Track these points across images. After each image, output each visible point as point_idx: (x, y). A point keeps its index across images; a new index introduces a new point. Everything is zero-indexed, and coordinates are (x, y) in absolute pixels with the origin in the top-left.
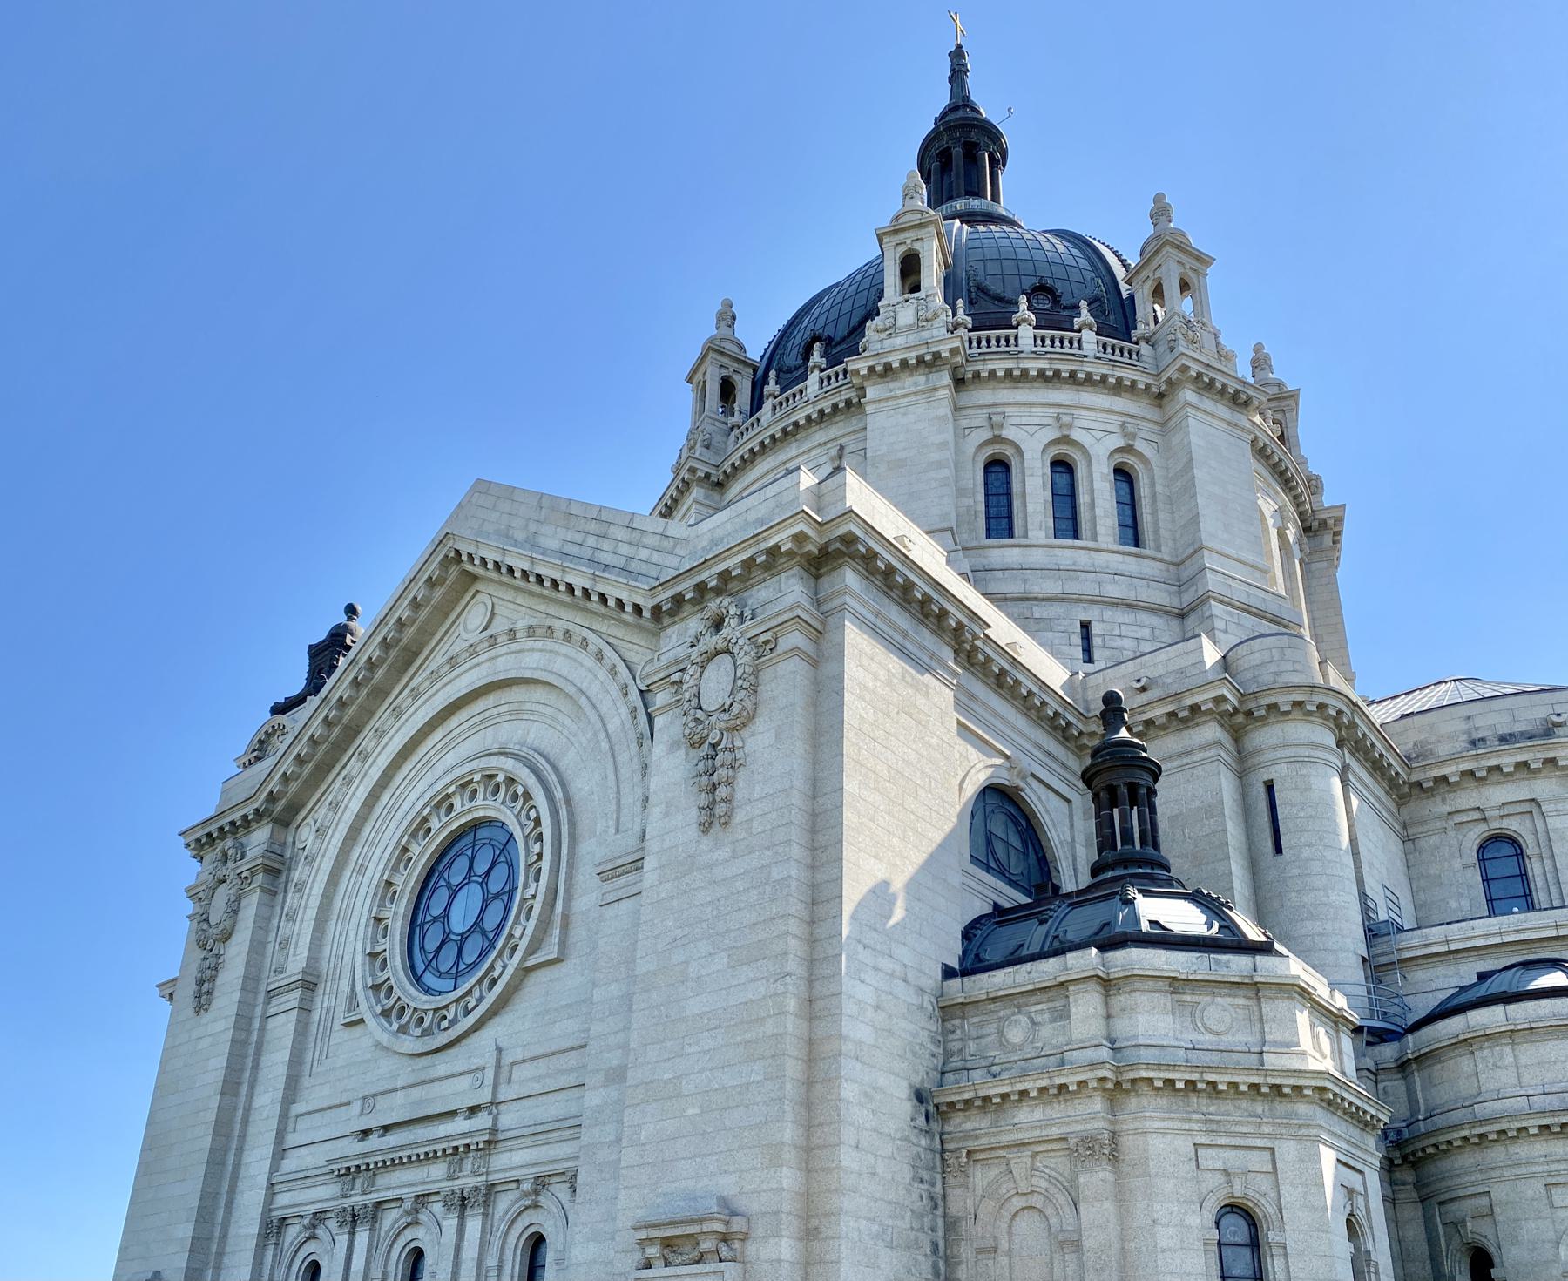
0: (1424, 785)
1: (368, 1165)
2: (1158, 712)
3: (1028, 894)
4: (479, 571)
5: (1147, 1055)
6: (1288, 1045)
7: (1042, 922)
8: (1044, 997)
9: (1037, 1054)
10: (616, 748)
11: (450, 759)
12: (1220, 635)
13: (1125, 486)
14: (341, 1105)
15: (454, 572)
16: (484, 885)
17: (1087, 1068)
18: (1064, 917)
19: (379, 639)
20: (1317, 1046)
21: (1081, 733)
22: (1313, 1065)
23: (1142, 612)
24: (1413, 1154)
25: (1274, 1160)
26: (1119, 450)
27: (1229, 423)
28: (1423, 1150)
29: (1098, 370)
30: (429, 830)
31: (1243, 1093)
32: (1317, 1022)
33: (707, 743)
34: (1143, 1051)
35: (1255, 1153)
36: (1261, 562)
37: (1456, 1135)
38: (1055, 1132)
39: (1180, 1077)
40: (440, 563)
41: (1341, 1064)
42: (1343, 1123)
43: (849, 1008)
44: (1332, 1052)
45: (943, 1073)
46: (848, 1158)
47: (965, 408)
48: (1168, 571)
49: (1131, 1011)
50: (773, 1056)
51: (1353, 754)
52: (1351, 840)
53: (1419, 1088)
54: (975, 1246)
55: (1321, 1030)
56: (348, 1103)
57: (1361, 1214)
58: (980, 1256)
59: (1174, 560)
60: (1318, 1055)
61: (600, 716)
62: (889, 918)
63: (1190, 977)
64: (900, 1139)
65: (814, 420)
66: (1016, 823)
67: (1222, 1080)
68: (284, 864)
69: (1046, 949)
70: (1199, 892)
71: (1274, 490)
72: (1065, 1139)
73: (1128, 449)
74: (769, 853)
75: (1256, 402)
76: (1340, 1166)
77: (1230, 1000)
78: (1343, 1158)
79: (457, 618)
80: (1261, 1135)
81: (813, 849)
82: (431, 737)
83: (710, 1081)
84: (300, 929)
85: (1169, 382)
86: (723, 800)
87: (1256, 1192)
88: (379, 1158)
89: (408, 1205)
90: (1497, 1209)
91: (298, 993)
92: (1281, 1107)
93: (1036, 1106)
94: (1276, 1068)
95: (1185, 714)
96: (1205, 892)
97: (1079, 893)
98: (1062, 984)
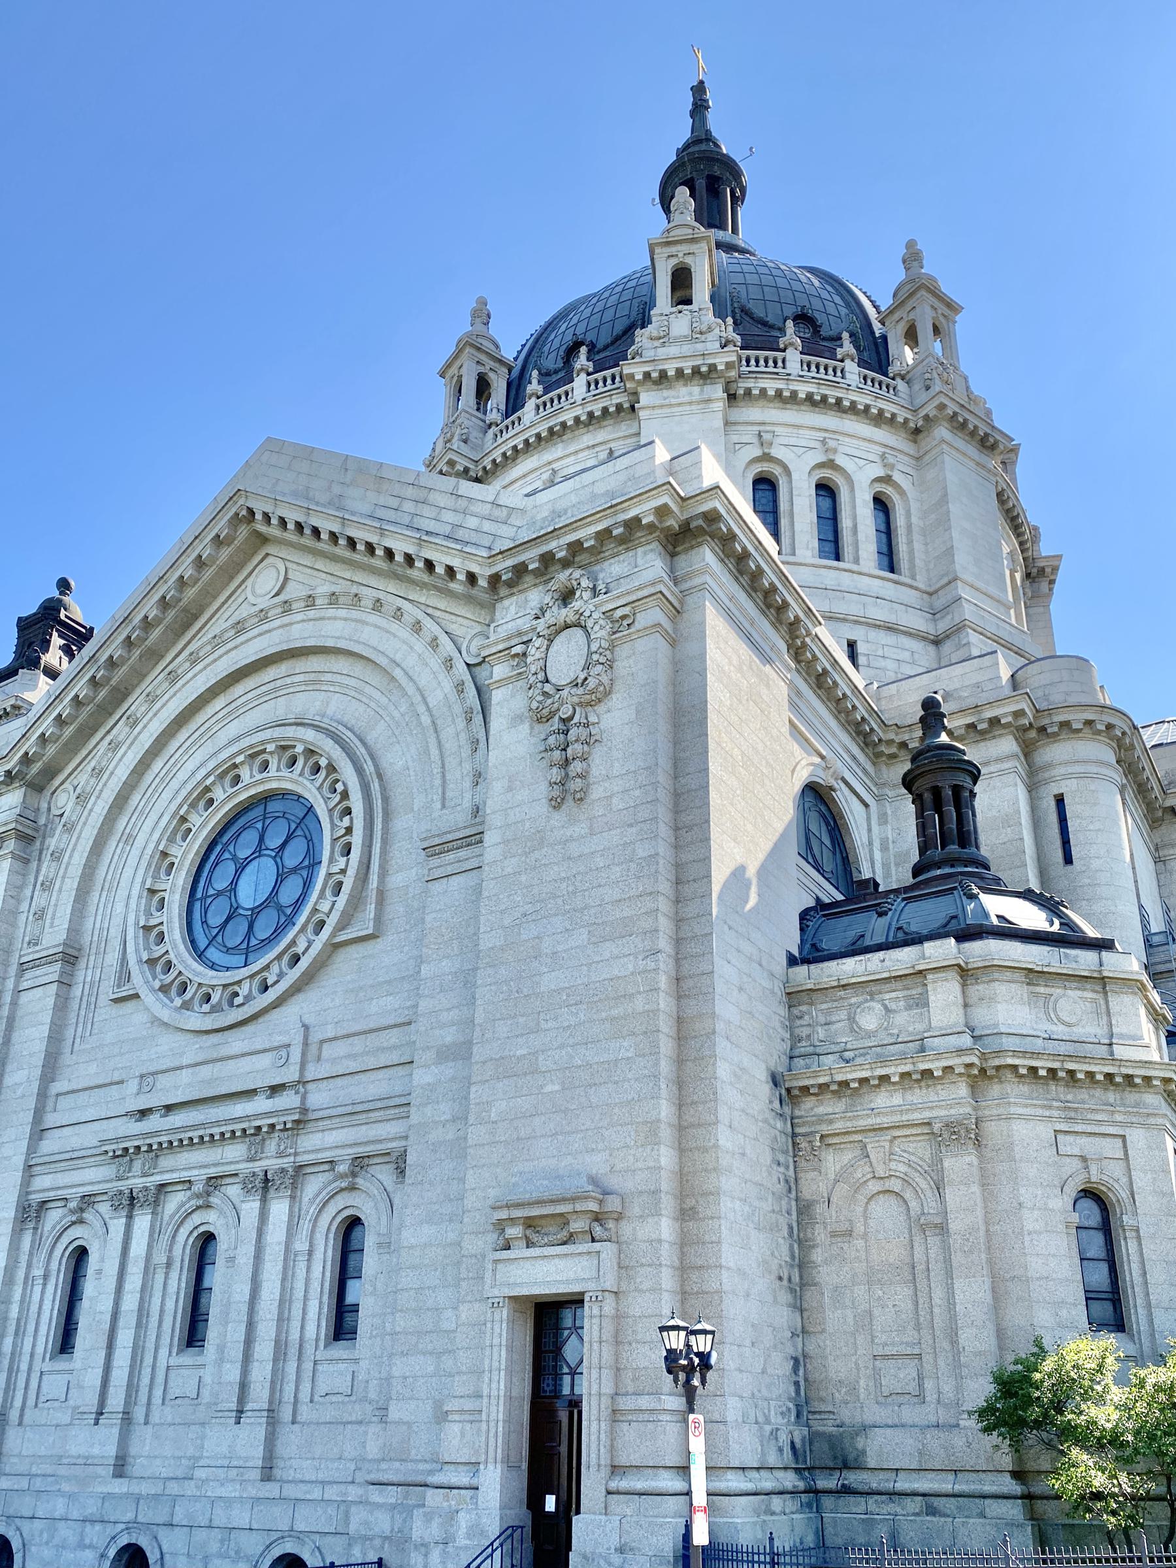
1: (150, 1145)
4: (274, 531)
5: (1009, 1043)
7: (880, 915)
8: (899, 985)
10: (438, 722)
11: (233, 729)
14: (111, 1084)
15: (243, 531)
16: (278, 860)
19: (157, 597)
26: (878, 480)
27: (978, 464)
29: (862, 400)
30: (211, 802)
31: (1099, 1082)
33: (556, 718)
34: (1004, 1039)
35: (1108, 1140)
38: (917, 1116)
40: (230, 521)
43: (720, 987)
45: (791, 1058)
46: (725, 1139)
47: (735, 424)
49: (992, 999)
50: (646, 1033)
54: (829, 1229)
56: (122, 1082)
61: (418, 689)
62: (746, 902)
65: (582, 422)
66: (827, 824)
67: (1080, 1068)
68: (37, 830)
69: (891, 940)
73: (887, 479)
74: (634, 830)
75: (1001, 447)
79: (243, 581)
80: (1114, 1123)
81: (677, 829)
82: (211, 705)
83: (572, 1057)
84: (57, 900)
85: (926, 418)
86: (578, 776)
88: (164, 1139)
89: (198, 1187)
91: (57, 966)
92: (1131, 1097)
93: (895, 1091)
98: (920, 972)
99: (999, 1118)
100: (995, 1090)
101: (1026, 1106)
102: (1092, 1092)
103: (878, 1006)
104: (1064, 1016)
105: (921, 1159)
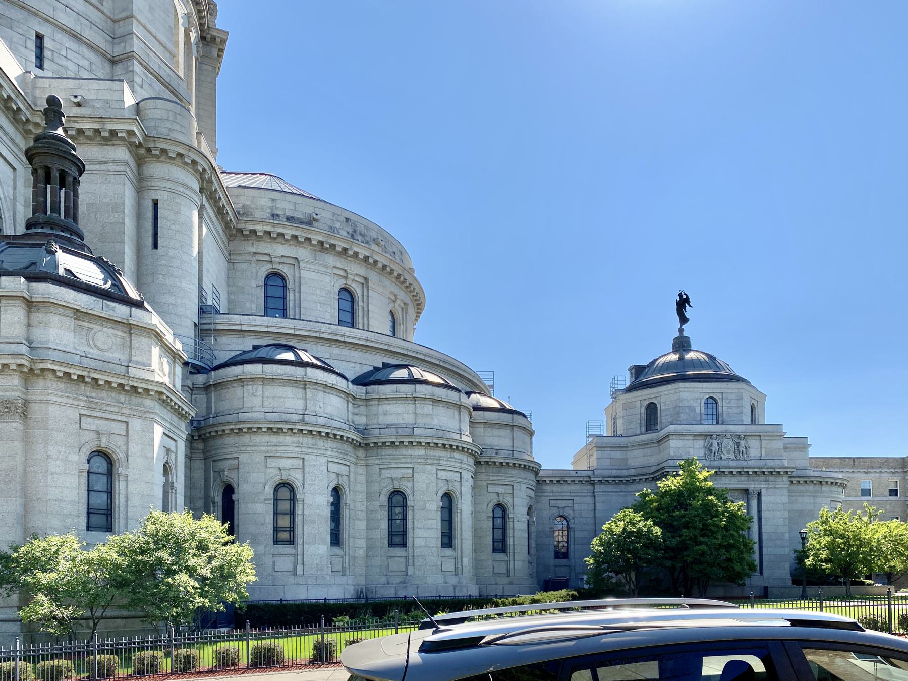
0: (244, 232)
6: (145, 365)
17: (10, 356)
21: (28, 120)
22: (157, 379)
28: (210, 433)
31: (114, 388)
32: (163, 355)
34: (51, 352)
37: (228, 427)
39: (75, 372)
41: (174, 381)
44: (169, 373)
52: (199, 253)
53: (213, 401)
55: (165, 360)
60: (161, 374)
63: (89, 312)
67: (102, 378)
77: (112, 331)
92: (136, 400)
94: (136, 377)
99: (41, 401)
100: (41, 383)
101: (61, 396)
102: (110, 393)
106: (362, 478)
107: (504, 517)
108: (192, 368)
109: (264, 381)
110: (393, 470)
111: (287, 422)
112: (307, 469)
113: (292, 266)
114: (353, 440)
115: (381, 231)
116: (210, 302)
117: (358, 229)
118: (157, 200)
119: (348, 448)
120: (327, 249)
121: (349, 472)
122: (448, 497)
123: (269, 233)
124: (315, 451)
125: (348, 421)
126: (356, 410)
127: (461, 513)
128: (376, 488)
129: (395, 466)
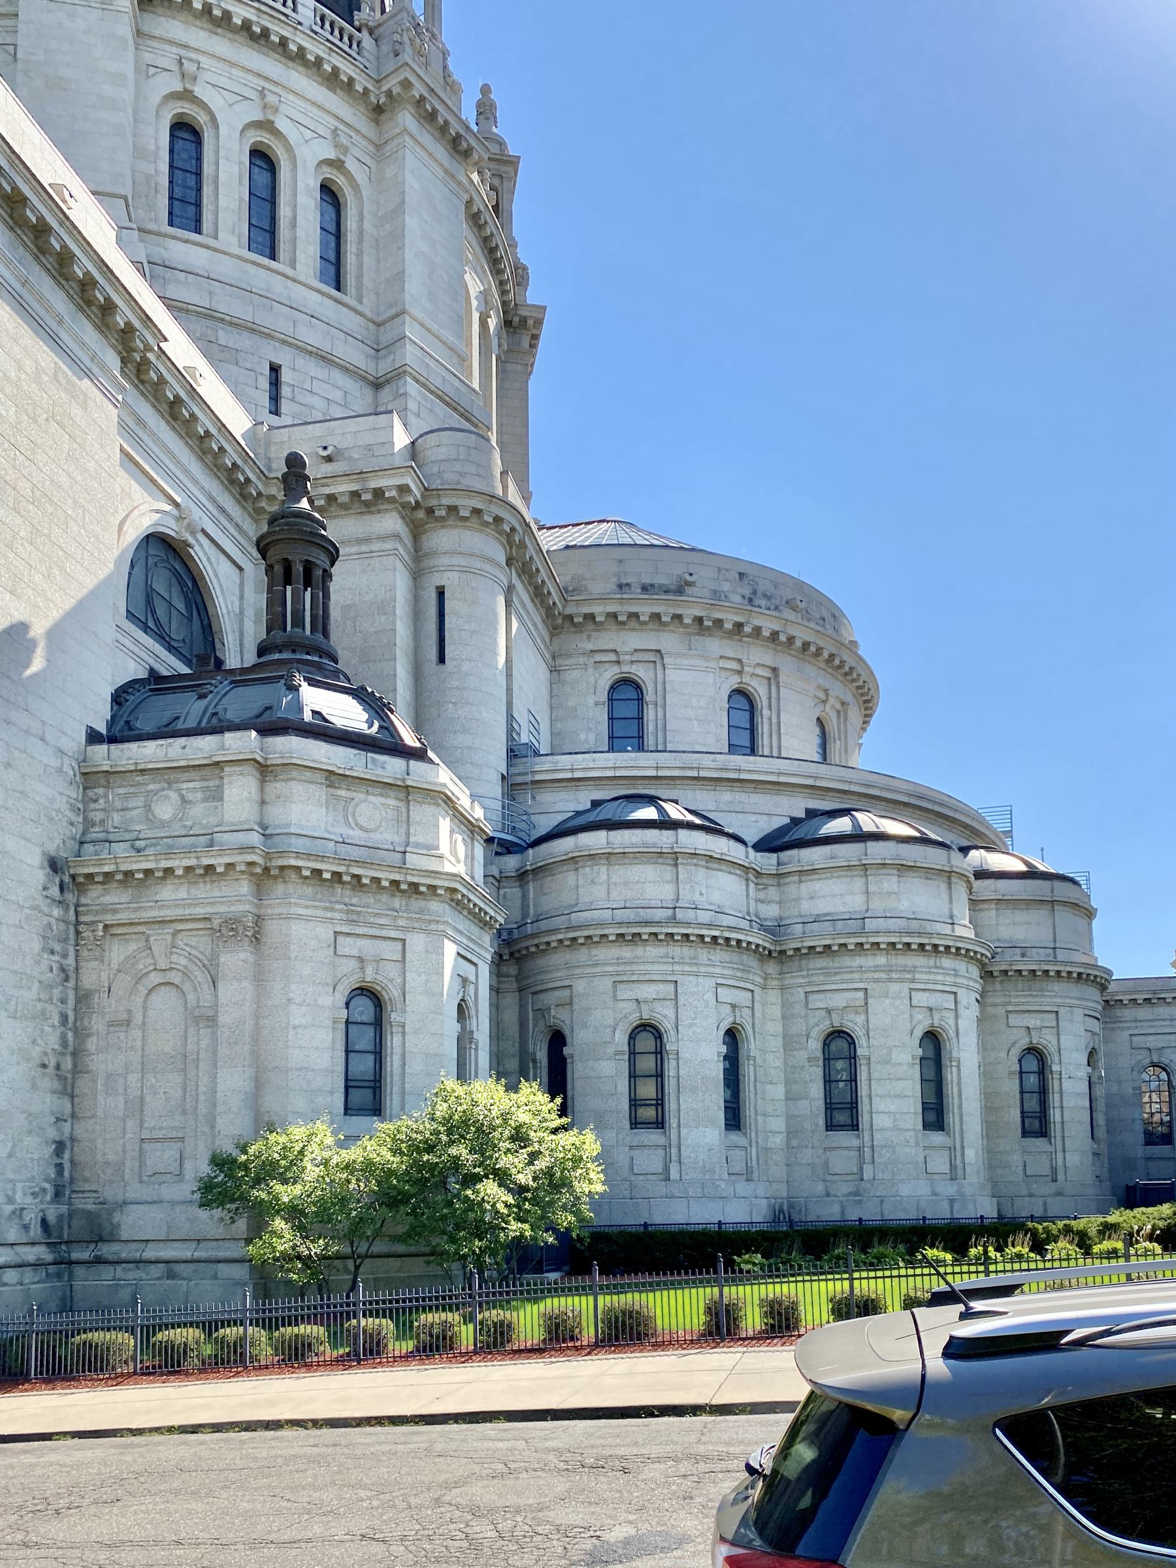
0: (576, 620)
2: (342, 488)
3: (188, 663)
6: (429, 848)
7: (202, 697)
9: (183, 833)
12: (412, 419)
13: (330, 211)
18: (225, 694)
20: (454, 852)
22: (448, 868)
23: (336, 370)
24: (519, 951)
25: (404, 949)
31: (384, 888)
32: (457, 830)
35: (389, 942)
36: (460, 346)
37: (554, 938)
38: (199, 911)
42: (467, 922)
44: (466, 857)
48: (367, 329)
51: (519, 576)
52: (507, 661)
55: (459, 838)
57: (470, 1001)
58: (112, 1029)
59: (375, 318)
60: (453, 860)
63: (347, 773)
64: (31, 908)
69: (203, 724)
70: (363, 688)
71: (482, 267)
72: (208, 919)
76: (460, 959)
77: (381, 800)
78: (463, 952)
80: (397, 928)
87: (386, 978)
90: (575, 1000)
93: (181, 884)
95: (367, 497)
96: (370, 690)
97: (243, 671)
102: (378, 897)
103: (173, 795)
104: (362, 821)
105: (202, 953)
106: (776, 1011)
107: (1043, 1071)
108: (500, 847)
109: (609, 857)
110: (829, 995)
111: (647, 923)
112: (681, 1000)
113: (652, 665)
114: (758, 946)
115: (800, 585)
116: (524, 739)
117: (761, 588)
118: (443, 587)
119: (750, 961)
120: (709, 628)
121: (753, 1001)
122: (933, 1040)
123: (614, 616)
124: (695, 969)
125: (748, 914)
126: (762, 895)
127: (958, 1067)
128: (799, 1027)
129: (833, 987)
